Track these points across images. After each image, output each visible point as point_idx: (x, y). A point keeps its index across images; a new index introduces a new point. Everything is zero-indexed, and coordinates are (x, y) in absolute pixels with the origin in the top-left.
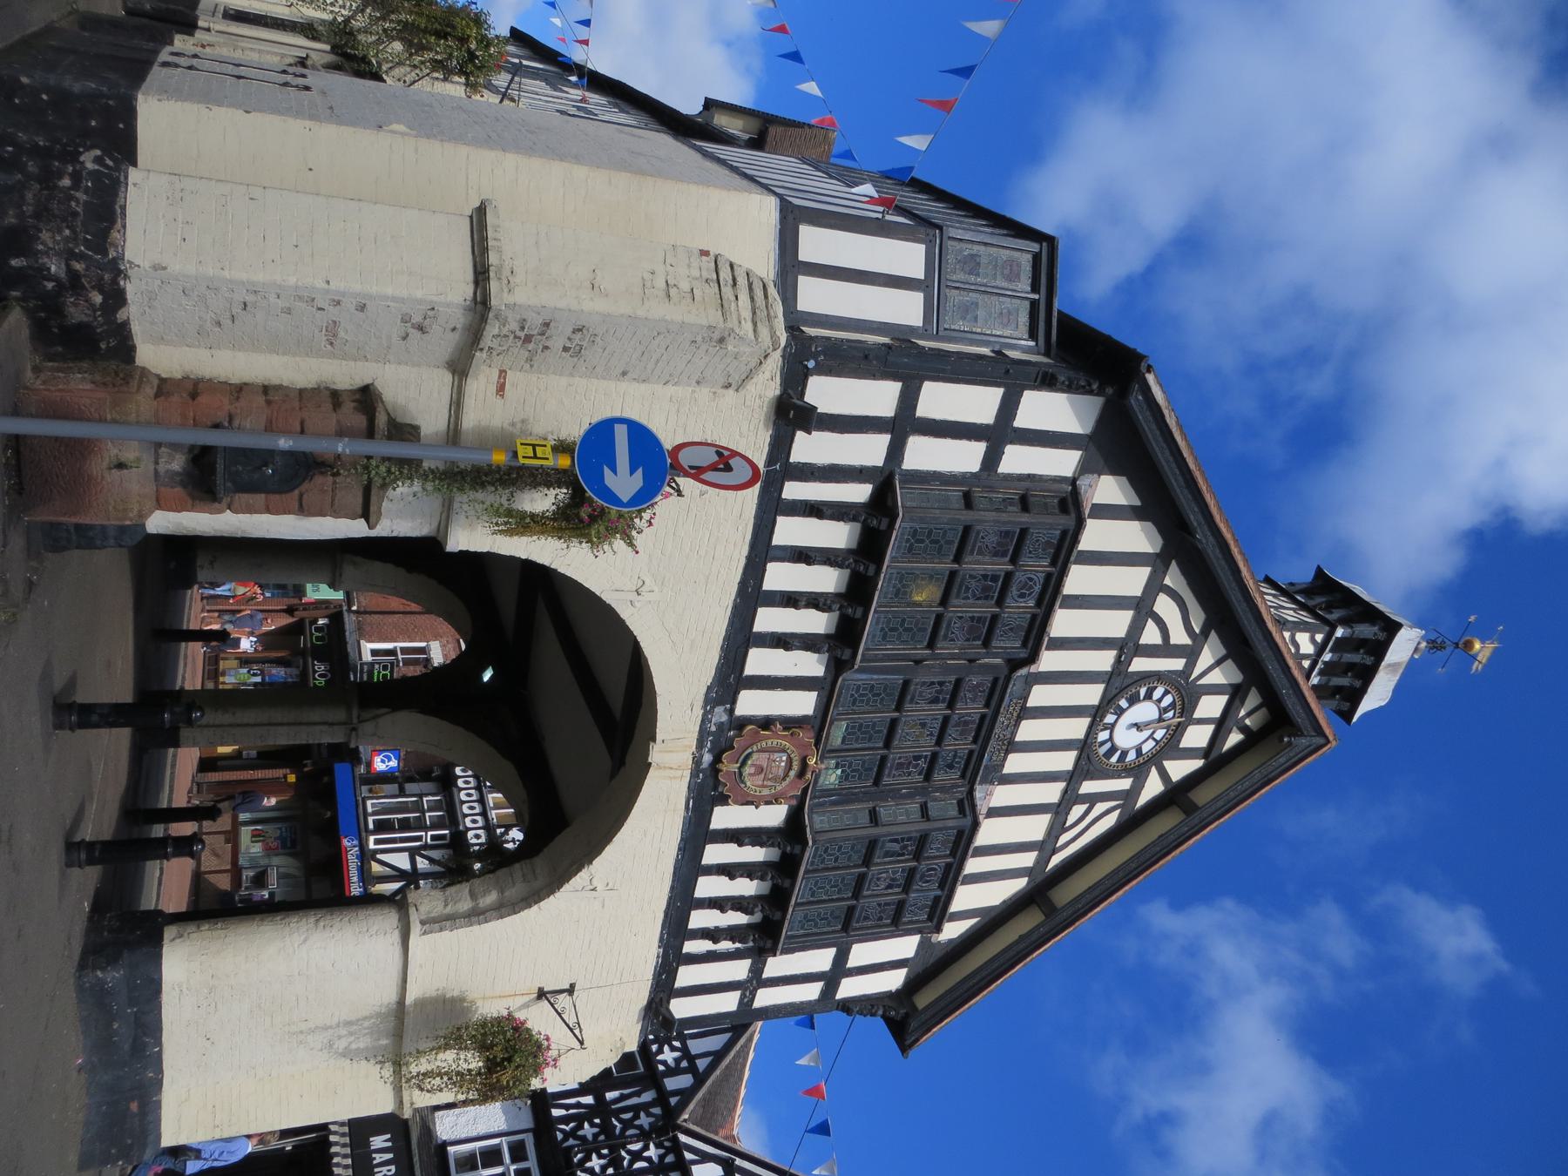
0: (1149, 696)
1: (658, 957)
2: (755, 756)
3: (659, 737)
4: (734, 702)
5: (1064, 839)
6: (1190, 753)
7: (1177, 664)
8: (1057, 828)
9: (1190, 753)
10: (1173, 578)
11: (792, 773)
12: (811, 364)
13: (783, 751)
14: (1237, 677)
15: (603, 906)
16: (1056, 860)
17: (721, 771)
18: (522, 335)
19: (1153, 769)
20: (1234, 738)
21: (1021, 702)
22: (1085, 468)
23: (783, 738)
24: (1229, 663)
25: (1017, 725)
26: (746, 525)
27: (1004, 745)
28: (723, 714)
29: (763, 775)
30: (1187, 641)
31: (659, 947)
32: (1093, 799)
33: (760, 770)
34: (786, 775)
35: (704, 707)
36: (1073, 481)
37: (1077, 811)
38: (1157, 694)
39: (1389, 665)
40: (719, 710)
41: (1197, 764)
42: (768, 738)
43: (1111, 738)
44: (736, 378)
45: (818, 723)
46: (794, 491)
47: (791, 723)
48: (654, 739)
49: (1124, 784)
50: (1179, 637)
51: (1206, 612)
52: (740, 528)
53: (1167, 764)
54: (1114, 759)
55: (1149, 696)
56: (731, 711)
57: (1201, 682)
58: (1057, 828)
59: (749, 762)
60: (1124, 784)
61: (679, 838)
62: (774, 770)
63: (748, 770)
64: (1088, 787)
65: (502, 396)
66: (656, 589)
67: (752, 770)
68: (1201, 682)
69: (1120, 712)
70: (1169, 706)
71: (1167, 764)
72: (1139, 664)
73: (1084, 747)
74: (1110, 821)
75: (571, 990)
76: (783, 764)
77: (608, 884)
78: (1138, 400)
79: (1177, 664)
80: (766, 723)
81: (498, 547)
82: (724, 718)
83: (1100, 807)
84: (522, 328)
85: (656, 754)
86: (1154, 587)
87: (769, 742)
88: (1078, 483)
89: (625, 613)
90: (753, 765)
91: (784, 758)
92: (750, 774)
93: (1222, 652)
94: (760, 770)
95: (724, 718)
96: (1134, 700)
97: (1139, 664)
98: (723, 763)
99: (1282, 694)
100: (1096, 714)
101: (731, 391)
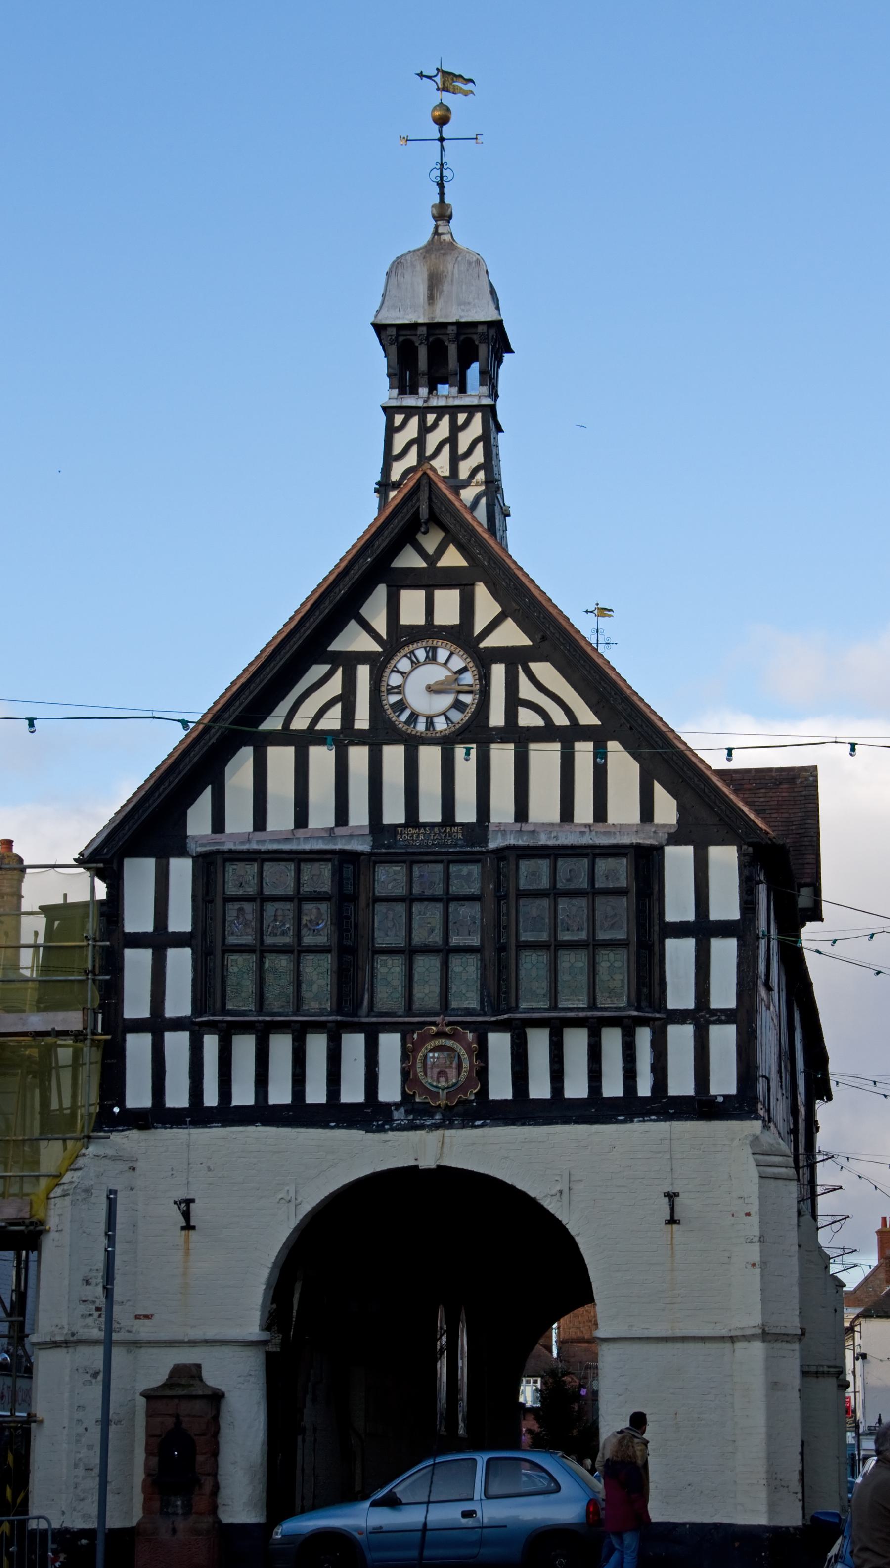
0: (399, 689)
1: (644, 1121)
2: (430, 1081)
3: (412, 1163)
4: (388, 1105)
5: (560, 719)
6: (467, 608)
7: (363, 672)
8: (548, 733)
9: (467, 608)
10: (273, 723)
11: (450, 1043)
12: (116, 1110)
13: (426, 1056)
14: (381, 592)
15: (581, 1181)
16: (587, 717)
17: (447, 1104)
18: (96, 1314)
19: (482, 645)
20: (453, 558)
21: (400, 829)
22: (182, 852)
23: (415, 1058)
24: (364, 611)
25: (425, 825)
26: (231, 1132)
27: (445, 831)
28: (399, 1111)
29: (447, 1070)
30: (340, 672)
31: (632, 1122)
32: (513, 701)
33: (442, 1073)
34: (450, 1049)
35: (385, 1131)
36: (193, 857)
37: (527, 718)
38: (395, 680)
39: (431, 298)
40: (396, 1115)
41: (481, 592)
42: (416, 1073)
43: (444, 714)
44: (124, 1166)
45: (405, 1031)
46: (211, 1099)
47: (406, 1055)
48: (416, 1167)
49: (498, 671)
50: (335, 686)
51: (310, 666)
52: (234, 1136)
53: (478, 629)
54: (467, 699)
55: (399, 689)
56: (397, 1105)
57: (383, 632)
58: (548, 733)
59: (435, 1084)
60: (498, 671)
61: (512, 1127)
62: (442, 1061)
63: (443, 1083)
64: (497, 718)
65: (152, 1315)
66: (287, 1188)
67: (442, 1080)
68: (383, 632)
69: (414, 717)
70: (410, 658)
71: (478, 629)
72: (362, 721)
73: (447, 743)
74: (544, 670)
75: (671, 1196)
76: (436, 1055)
77: (557, 1181)
78: (107, 851)
79: (363, 672)
80: (406, 1075)
81: (257, 1305)
82: (402, 1110)
83: (526, 690)
84: (90, 1315)
85: (427, 1163)
86: (285, 737)
87: (418, 1070)
88: (194, 855)
89: (307, 1207)
90: (438, 1082)
91: (431, 1055)
92: (447, 1081)
93: (353, 625)
94: (442, 1073)
95: (402, 1110)
96: (401, 706)
97: (362, 721)
98: (439, 1104)
99: (372, 562)
100: (412, 744)
101: (138, 1165)
